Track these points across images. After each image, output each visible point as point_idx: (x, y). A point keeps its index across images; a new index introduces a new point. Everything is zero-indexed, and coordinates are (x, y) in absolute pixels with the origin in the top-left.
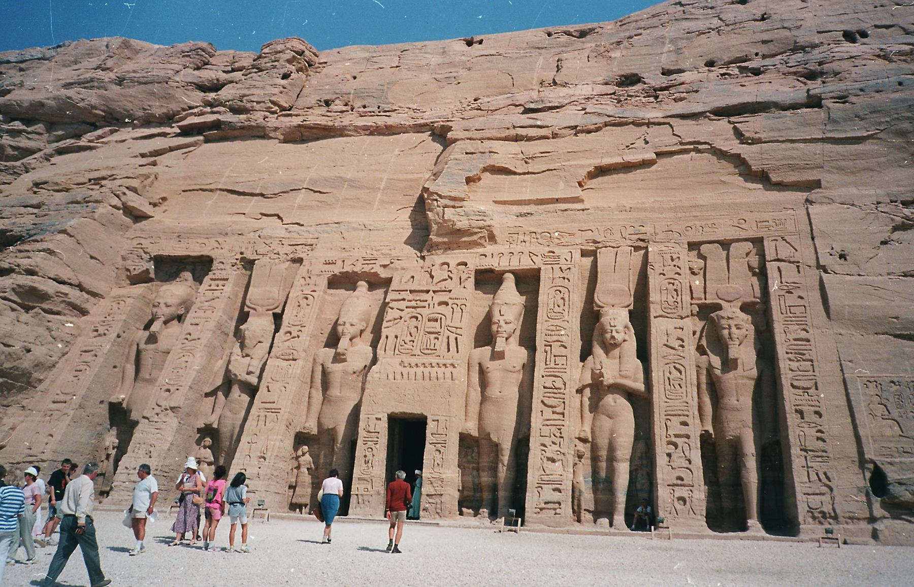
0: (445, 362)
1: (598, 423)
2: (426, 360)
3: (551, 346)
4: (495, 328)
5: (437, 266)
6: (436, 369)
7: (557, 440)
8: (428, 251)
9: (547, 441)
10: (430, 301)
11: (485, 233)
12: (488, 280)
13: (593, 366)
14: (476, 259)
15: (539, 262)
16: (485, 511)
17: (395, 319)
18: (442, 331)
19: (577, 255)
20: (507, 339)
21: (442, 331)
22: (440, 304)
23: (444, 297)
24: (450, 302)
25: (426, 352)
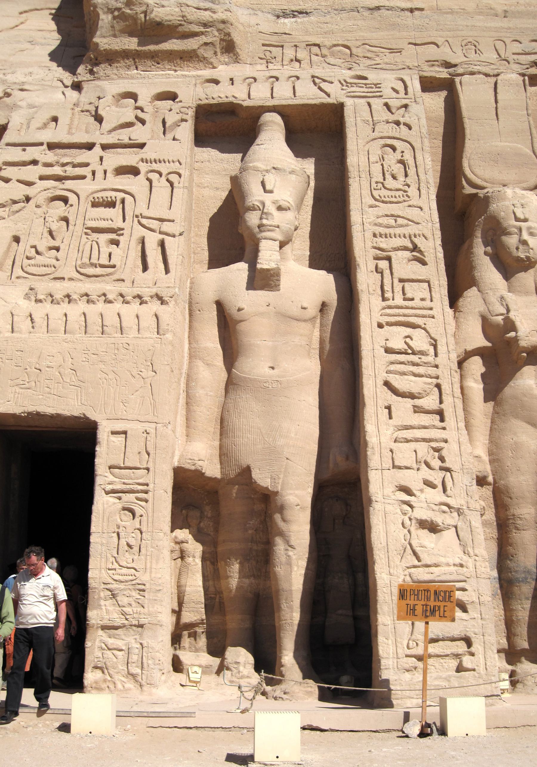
0: (137, 291)
1: (508, 439)
2: (92, 287)
3: (389, 259)
4: (252, 219)
5: (109, 98)
6: (118, 306)
7: (436, 477)
8: (91, 72)
9: (412, 479)
10: (95, 165)
11: (213, 36)
12: (226, 127)
13: (482, 308)
14: (192, 86)
15: (336, 94)
16: (241, 657)
17: (15, 202)
18: (126, 225)
19: (415, 85)
20: (282, 245)
21: (126, 225)
22: (121, 171)
23: (128, 158)
24: (143, 168)
25: (91, 271)
